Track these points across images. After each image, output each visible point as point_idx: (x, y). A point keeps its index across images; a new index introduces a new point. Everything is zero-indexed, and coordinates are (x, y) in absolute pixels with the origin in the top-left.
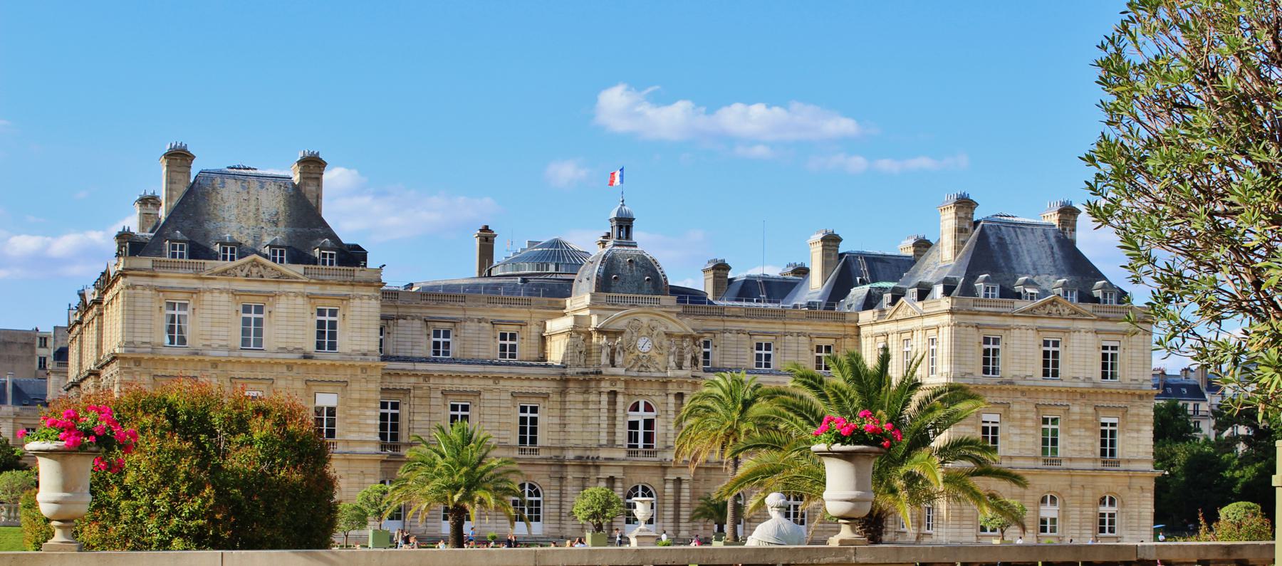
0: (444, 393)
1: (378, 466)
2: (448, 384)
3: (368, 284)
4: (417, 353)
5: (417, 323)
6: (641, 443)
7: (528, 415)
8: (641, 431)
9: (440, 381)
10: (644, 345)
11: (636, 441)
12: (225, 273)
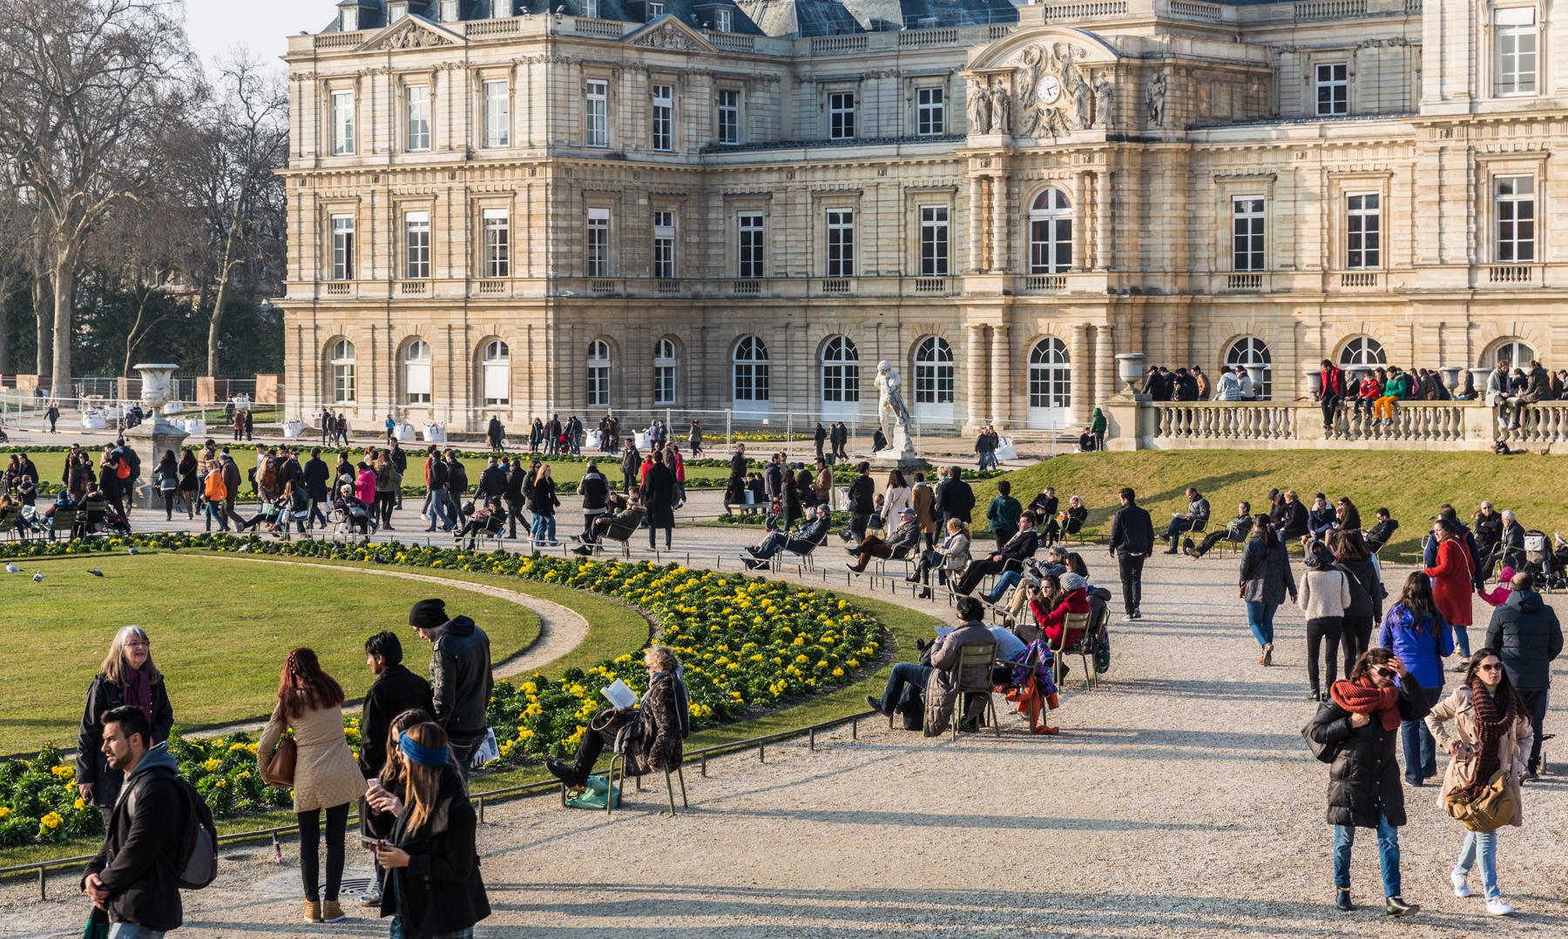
0: (818, 196)
1: (551, 314)
2: (819, 180)
3: (532, 40)
4: (891, 131)
5: (890, 84)
6: (1052, 264)
7: (935, 224)
8: (1052, 242)
9: (809, 178)
10: (1049, 90)
11: (1045, 261)
12: (378, 45)
